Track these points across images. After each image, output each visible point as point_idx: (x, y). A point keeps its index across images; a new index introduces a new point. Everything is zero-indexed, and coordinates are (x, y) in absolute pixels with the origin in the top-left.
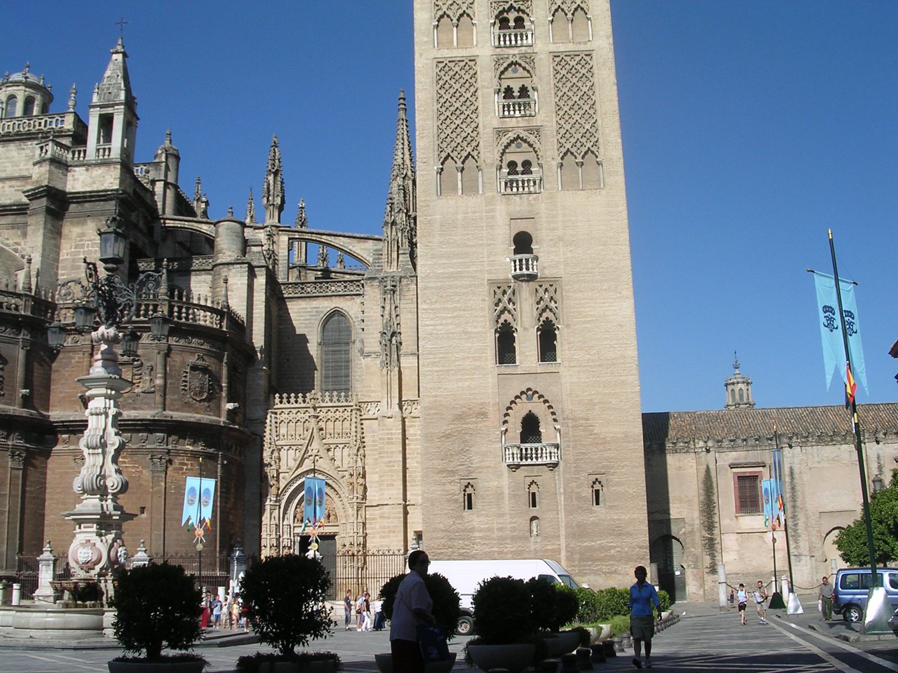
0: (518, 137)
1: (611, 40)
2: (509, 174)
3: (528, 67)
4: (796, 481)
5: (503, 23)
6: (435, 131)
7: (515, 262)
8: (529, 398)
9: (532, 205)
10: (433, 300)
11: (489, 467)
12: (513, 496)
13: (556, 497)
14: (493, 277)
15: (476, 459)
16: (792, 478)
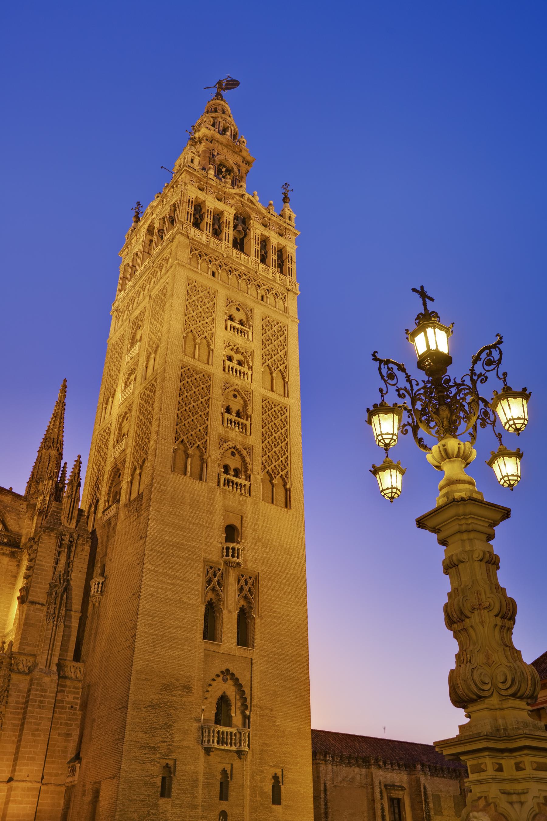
0: (234, 448)
1: (300, 403)
2: (224, 472)
3: (245, 398)
4: (328, 797)
5: (230, 359)
6: (176, 417)
7: (228, 549)
8: (225, 681)
9: (242, 505)
10: (158, 563)
11: (188, 748)
12: (207, 785)
13: (243, 790)
14: (209, 557)
15: (177, 737)
16: (326, 794)
